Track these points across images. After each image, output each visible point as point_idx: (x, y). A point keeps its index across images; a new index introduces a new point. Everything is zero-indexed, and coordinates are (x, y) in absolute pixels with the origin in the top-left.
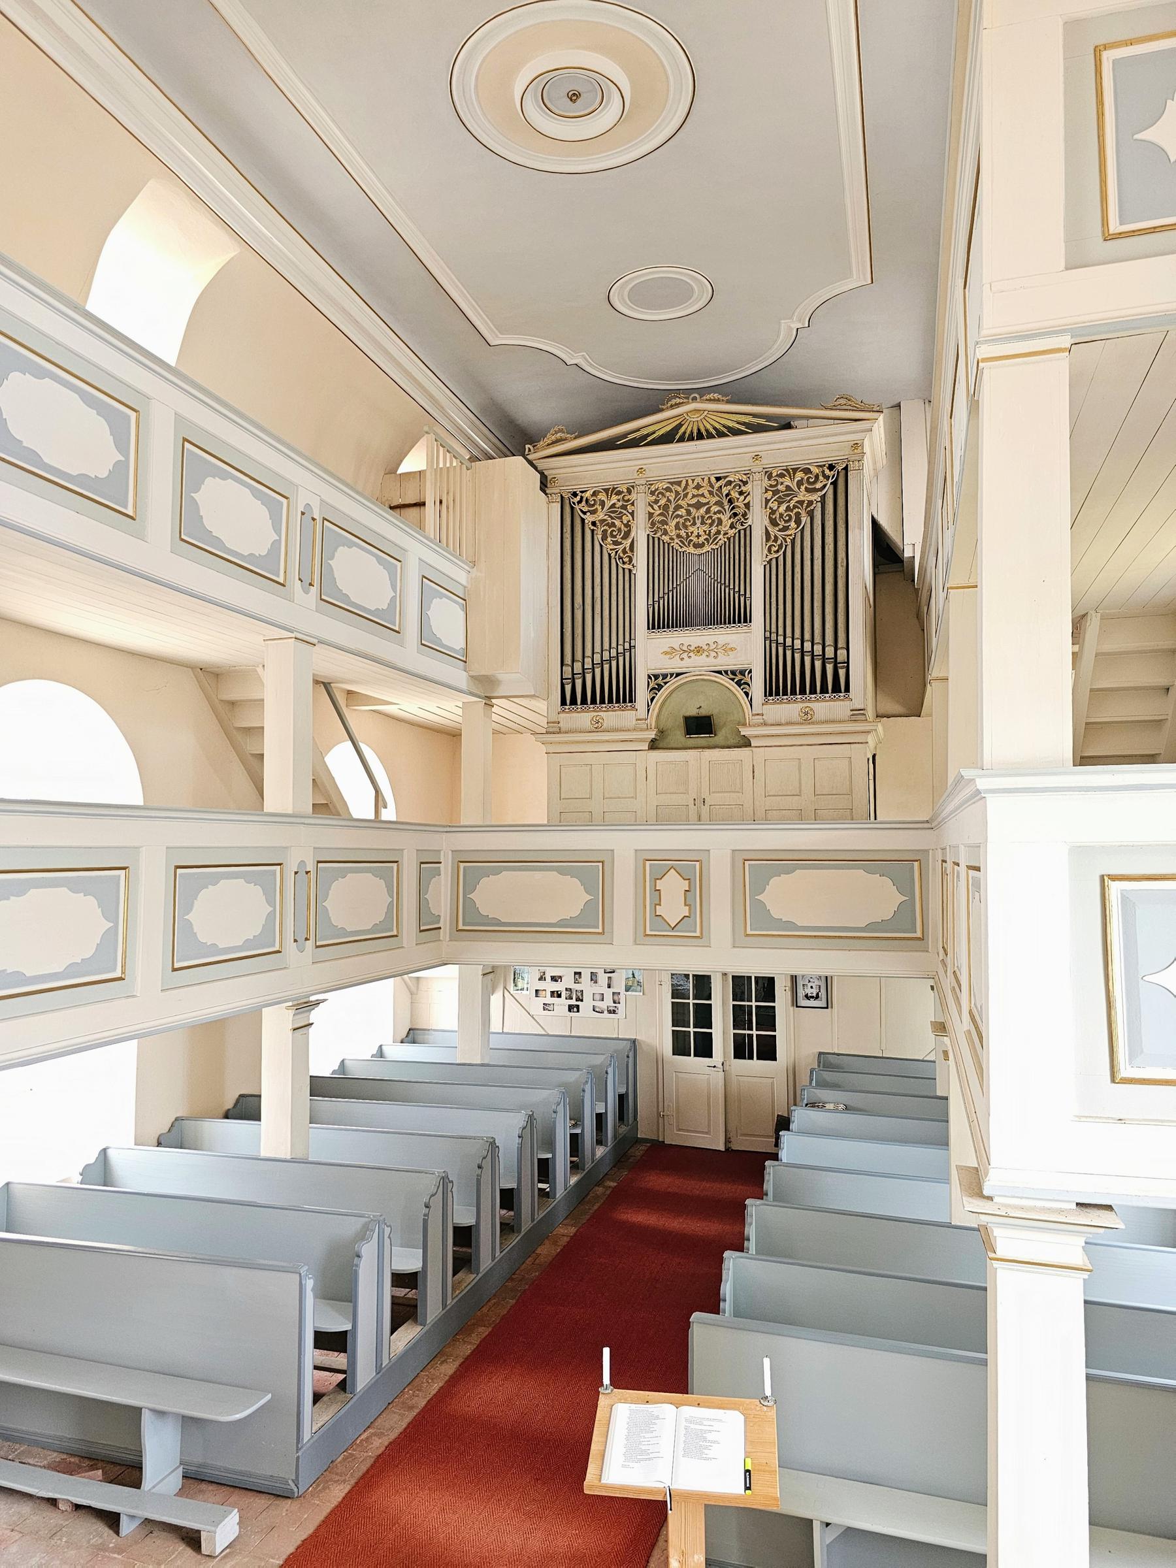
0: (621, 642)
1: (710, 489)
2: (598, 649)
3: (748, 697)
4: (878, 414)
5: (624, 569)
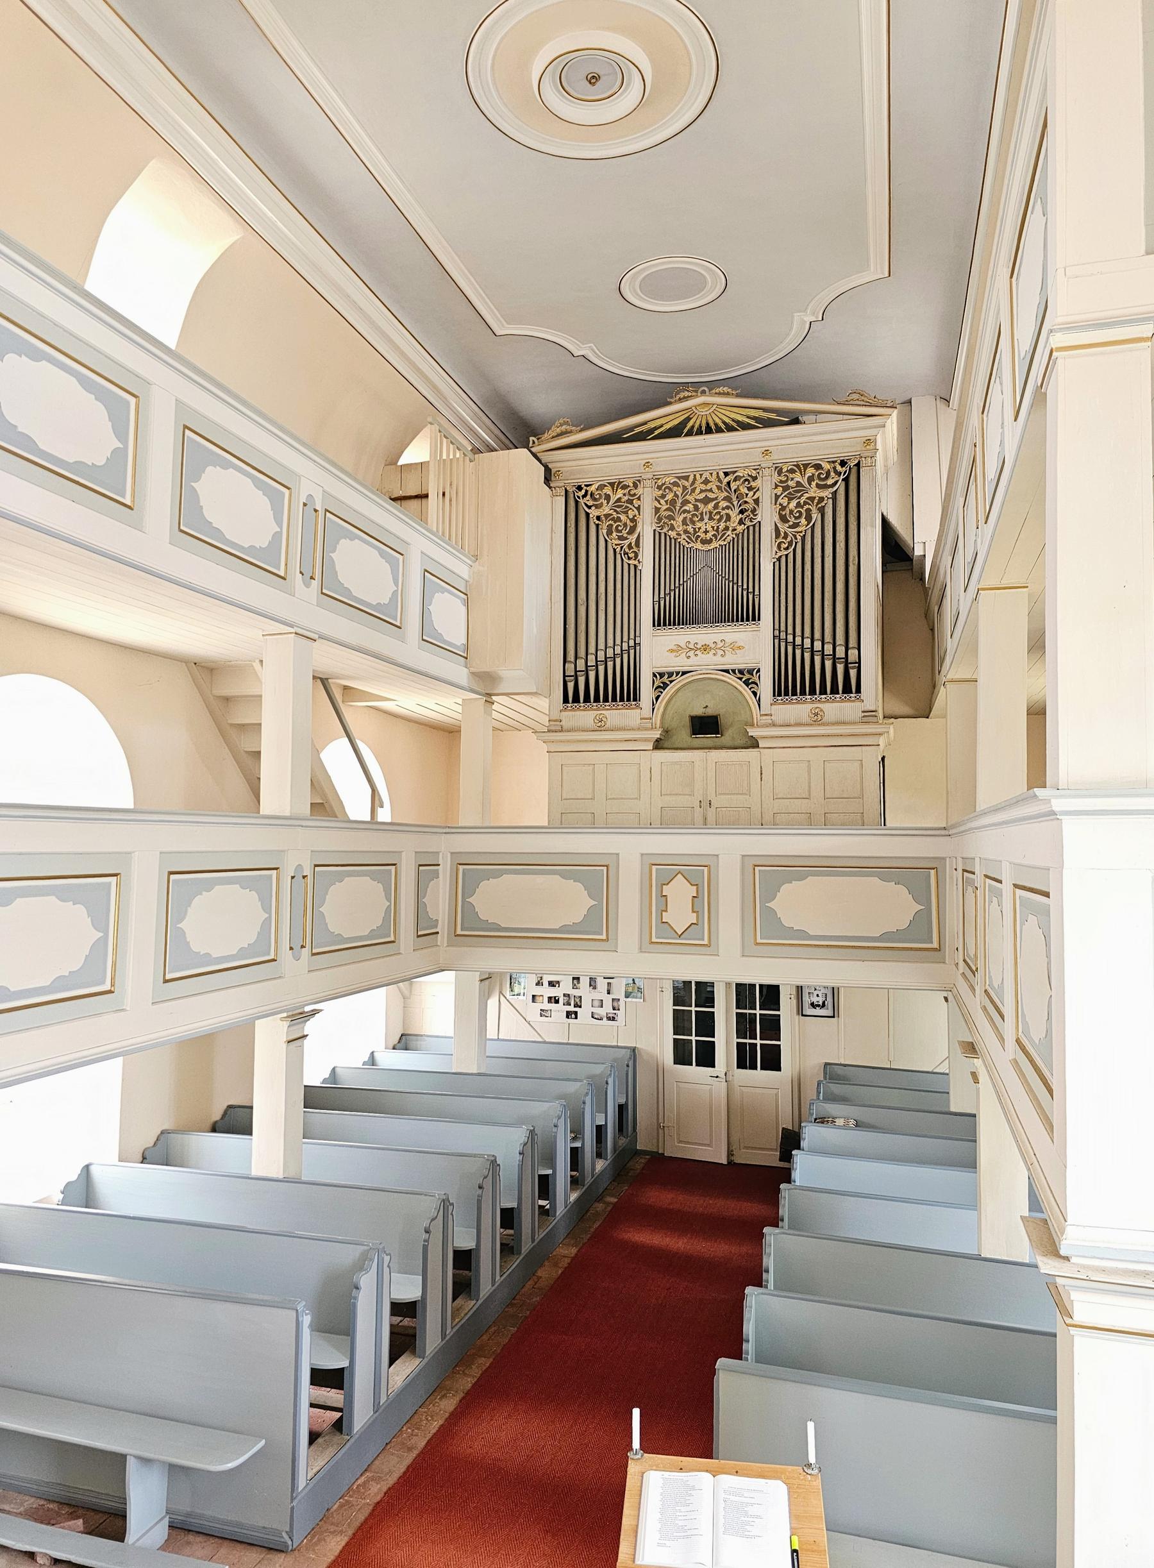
0: (625, 639)
1: (719, 484)
2: (601, 646)
3: (756, 697)
4: (892, 410)
5: (629, 565)
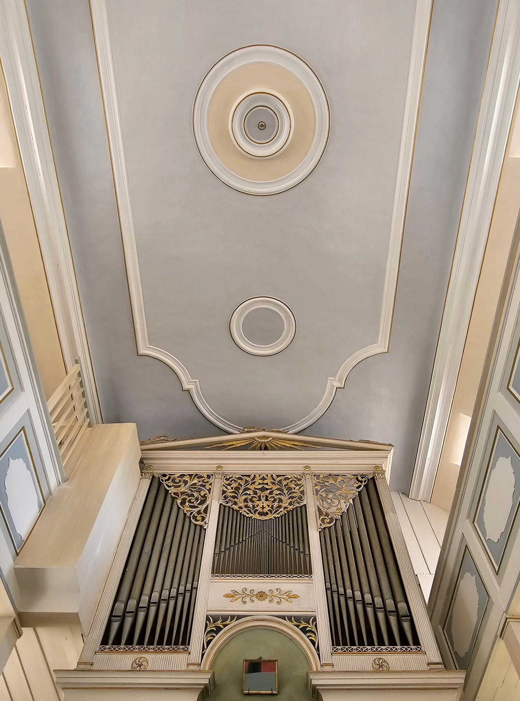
1: (273, 481)
3: (314, 645)
